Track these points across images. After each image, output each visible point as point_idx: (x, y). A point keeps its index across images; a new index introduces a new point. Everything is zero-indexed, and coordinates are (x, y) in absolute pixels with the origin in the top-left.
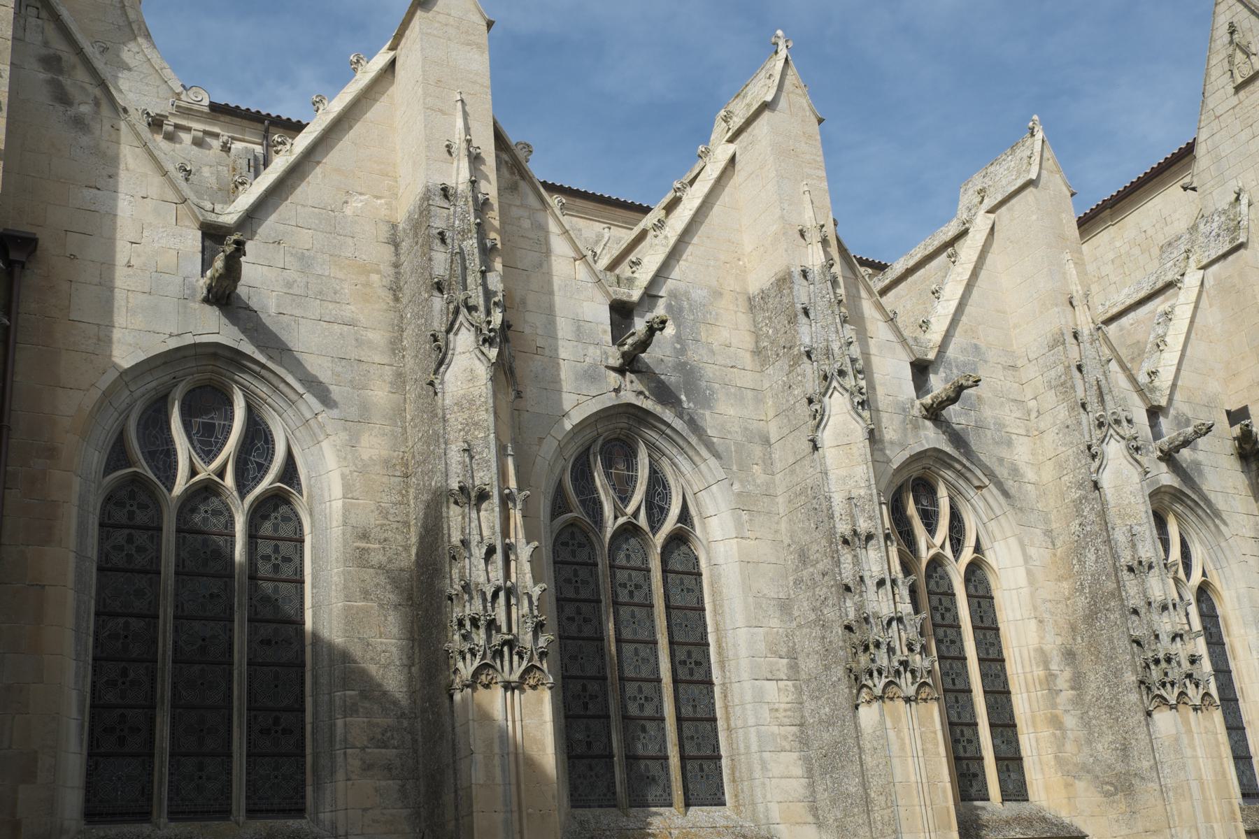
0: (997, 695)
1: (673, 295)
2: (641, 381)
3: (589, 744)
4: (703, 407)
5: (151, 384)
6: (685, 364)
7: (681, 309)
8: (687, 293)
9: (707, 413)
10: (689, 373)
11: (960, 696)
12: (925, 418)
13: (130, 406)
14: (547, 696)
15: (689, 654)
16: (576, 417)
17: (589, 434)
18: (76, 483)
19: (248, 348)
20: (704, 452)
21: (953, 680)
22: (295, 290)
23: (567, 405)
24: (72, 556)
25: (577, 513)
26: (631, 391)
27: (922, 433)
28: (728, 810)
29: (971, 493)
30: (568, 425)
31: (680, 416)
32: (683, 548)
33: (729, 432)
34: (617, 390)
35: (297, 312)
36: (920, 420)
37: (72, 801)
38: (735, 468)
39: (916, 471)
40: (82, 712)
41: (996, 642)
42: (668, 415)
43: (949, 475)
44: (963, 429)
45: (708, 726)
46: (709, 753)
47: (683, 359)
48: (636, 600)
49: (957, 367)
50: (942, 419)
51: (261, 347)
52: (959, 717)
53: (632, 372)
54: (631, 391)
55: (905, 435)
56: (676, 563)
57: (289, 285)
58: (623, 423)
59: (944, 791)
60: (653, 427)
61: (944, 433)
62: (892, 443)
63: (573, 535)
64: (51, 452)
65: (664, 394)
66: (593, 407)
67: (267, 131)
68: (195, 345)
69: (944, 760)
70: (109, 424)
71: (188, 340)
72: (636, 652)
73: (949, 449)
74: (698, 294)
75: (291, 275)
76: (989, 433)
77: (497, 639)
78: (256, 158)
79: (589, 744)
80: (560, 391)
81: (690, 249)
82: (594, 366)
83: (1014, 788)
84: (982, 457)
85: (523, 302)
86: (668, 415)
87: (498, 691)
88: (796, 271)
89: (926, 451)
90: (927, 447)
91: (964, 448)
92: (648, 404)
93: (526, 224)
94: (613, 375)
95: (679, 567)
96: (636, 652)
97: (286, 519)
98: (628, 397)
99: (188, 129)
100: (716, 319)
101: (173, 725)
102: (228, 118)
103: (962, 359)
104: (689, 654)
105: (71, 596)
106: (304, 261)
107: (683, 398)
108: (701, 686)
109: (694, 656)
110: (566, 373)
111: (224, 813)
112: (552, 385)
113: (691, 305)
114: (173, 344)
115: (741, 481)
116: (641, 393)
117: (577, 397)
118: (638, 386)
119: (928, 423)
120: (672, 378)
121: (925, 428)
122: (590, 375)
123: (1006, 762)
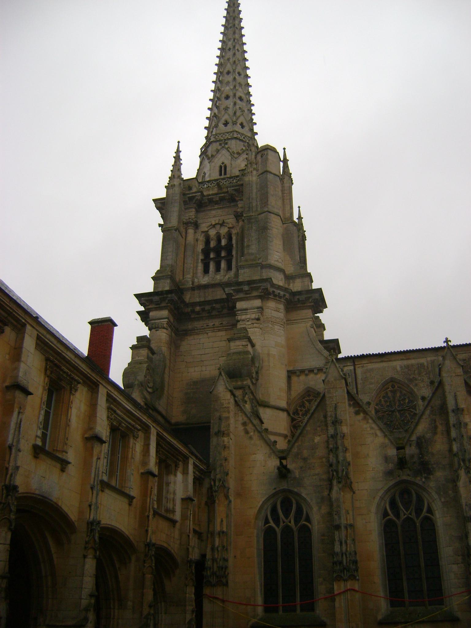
113: (425, 440)
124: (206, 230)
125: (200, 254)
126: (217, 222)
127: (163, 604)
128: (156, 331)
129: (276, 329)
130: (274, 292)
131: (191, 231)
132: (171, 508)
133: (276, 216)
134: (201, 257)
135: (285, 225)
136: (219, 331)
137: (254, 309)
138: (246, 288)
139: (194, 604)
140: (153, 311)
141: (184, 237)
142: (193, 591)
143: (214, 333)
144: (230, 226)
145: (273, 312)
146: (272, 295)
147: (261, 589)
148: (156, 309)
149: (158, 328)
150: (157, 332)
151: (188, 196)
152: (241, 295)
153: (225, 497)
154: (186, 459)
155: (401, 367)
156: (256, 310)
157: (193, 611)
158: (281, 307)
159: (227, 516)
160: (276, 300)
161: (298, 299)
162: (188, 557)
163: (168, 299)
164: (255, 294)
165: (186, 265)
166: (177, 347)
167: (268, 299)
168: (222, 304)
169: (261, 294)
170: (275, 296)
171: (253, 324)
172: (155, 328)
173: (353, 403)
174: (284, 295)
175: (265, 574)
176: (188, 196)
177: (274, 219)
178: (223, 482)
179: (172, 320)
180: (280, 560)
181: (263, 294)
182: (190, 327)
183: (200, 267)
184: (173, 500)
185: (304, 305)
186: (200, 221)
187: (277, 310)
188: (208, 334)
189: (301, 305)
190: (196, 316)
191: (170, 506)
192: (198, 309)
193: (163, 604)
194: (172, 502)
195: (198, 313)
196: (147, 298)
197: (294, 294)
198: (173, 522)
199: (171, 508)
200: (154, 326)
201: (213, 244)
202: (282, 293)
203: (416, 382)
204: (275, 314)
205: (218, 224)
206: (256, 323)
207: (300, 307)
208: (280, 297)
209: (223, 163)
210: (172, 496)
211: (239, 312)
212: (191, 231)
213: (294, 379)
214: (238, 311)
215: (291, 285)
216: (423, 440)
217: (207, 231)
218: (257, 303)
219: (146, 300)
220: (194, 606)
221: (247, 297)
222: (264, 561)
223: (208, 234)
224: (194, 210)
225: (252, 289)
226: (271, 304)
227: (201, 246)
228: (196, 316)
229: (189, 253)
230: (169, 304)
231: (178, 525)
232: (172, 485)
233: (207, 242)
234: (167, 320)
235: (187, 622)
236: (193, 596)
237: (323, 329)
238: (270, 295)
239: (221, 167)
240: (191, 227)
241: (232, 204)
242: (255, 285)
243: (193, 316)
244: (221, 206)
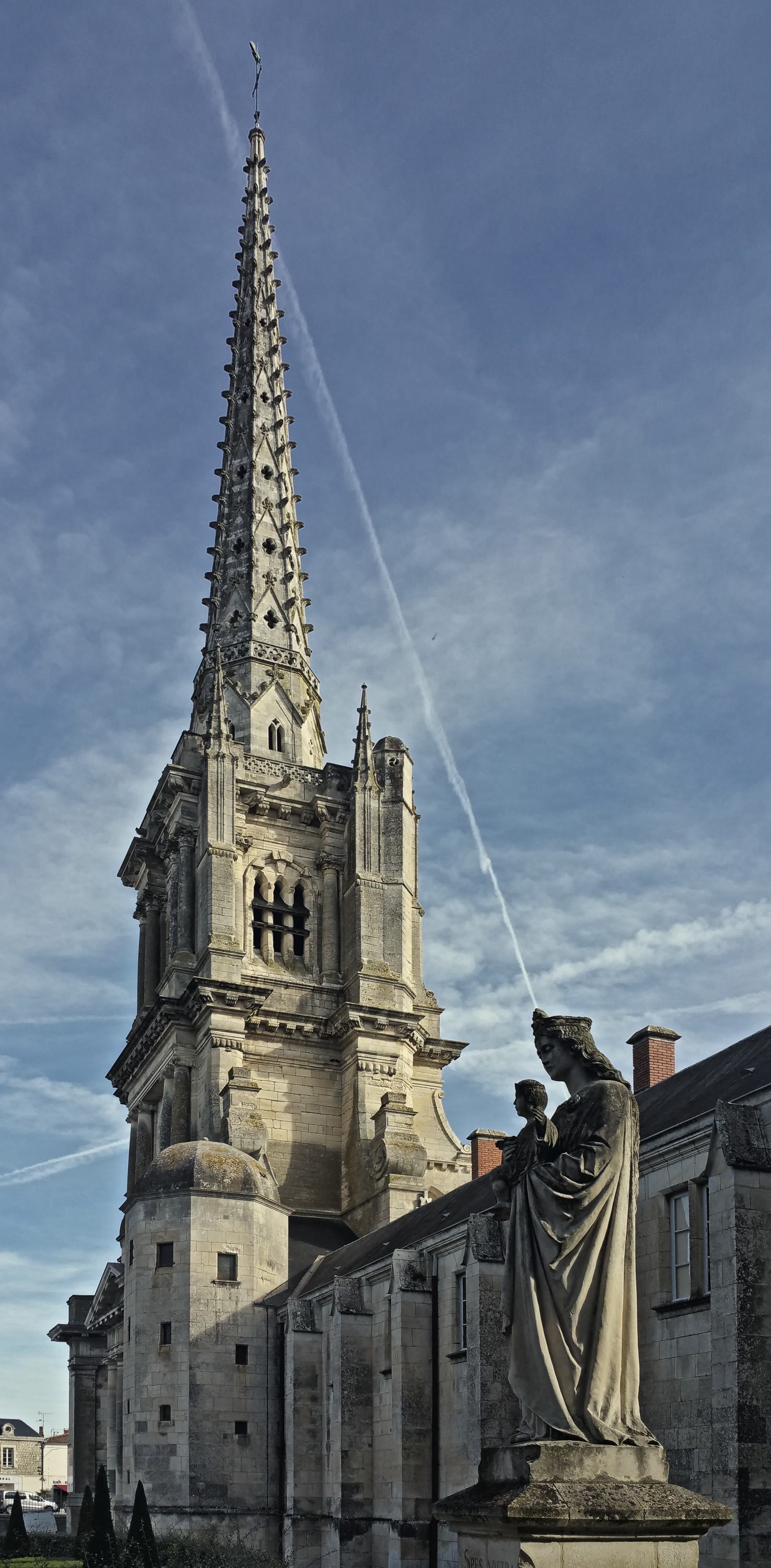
136: (301, 1067)
137: (386, 1056)
138: (382, 1020)
140: (217, 1012)
143: (292, 1068)
148: (225, 1012)
149: (232, 1047)
156: (389, 1058)
168: (318, 1027)
188: (281, 1067)
192: (274, 1022)
195: (272, 1029)
196: (214, 990)
209: (276, 722)
221: (376, 1034)
239: (271, 729)
241: (309, 829)
242: (396, 1020)
243: (259, 1032)
244: (290, 826)
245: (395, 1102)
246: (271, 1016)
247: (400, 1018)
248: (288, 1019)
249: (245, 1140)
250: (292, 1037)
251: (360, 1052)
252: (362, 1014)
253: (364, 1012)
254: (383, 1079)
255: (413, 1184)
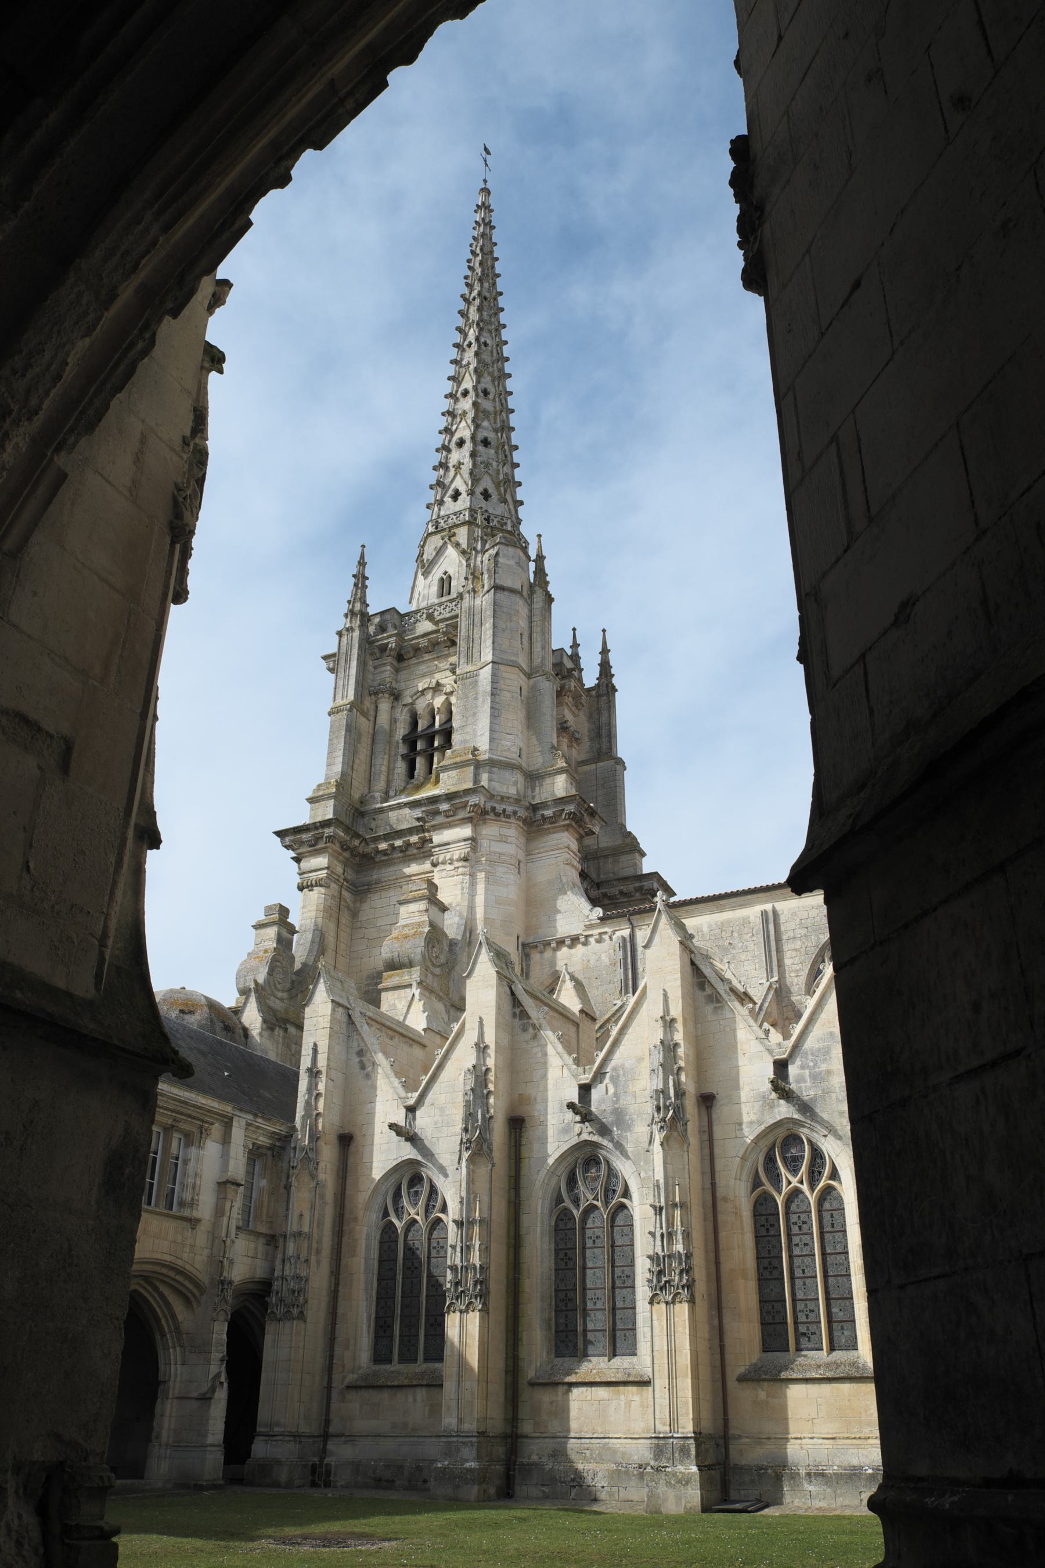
0: (839, 1278)
1: (615, 1069)
2: (591, 1127)
3: (566, 1325)
4: (626, 1132)
5: (393, 1180)
6: (618, 1109)
7: (618, 1076)
8: (622, 1066)
9: (628, 1134)
10: (619, 1114)
11: (808, 1281)
12: (780, 1098)
13: (387, 1192)
14: (477, 1314)
15: (623, 1272)
16: (556, 1155)
17: (570, 1159)
18: (365, 1230)
19: (420, 1158)
20: (623, 1159)
21: (803, 1271)
22: (439, 1125)
23: (550, 1150)
24: (363, 1261)
25: (568, 1203)
26: (588, 1133)
27: (776, 1110)
28: (634, 1359)
29: (823, 1139)
30: (551, 1161)
31: (612, 1141)
32: (625, 1211)
33: (640, 1142)
34: (579, 1134)
35: (439, 1135)
36: (776, 1101)
37: (365, 1356)
38: (642, 1164)
39: (781, 1133)
40: (369, 1320)
41: (843, 1241)
42: (605, 1142)
43: (805, 1131)
44: (811, 1099)
45: (630, 1311)
46: (630, 1327)
47: (616, 1106)
48: (596, 1245)
49: (812, 1054)
50: (795, 1095)
51: (423, 1156)
52: (805, 1293)
53: (588, 1121)
54: (588, 1133)
55: (763, 1115)
56: (620, 1220)
57: (436, 1123)
58: (589, 1149)
59: (686, 1355)
60: (602, 1149)
61: (794, 1106)
62: (751, 1122)
63: (565, 1215)
64: (356, 1219)
65: (604, 1130)
66: (565, 1147)
67: (629, 920)
68: (402, 1161)
69: (688, 1337)
70: (379, 1200)
71: (400, 1160)
72: (594, 1274)
73: (796, 1116)
74: (628, 1064)
75: (437, 1118)
76: (834, 1096)
77: (460, 1289)
78: (624, 939)
79: (566, 1325)
80: (547, 1143)
81: (627, 1036)
82: (569, 1124)
83: (846, 1341)
84: (825, 1116)
85: (535, 1099)
86: (605, 1142)
87: (458, 1314)
88: (651, 1046)
89: (780, 1120)
90: (779, 1118)
91: (810, 1112)
92: (596, 1138)
93: (539, 1055)
94: (578, 1125)
95: (622, 1223)
96: (594, 1274)
97: (442, 1229)
98: (585, 1137)
99: (592, 935)
100: (639, 1075)
101: (401, 1324)
102: (610, 921)
103: (817, 1046)
104: (623, 1272)
105: (362, 1277)
106: (442, 1109)
107: (615, 1129)
108: (629, 1289)
109: (626, 1272)
110: (551, 1132)
111: (415, 1360)
112: (544, 1140)
114: (395, 1163)
115: (645, 1171)
116: (592, 1132)
117: (557, 1144)
118: (590, 1129)
119: (782, 1102)
120: (608, 1119)
121: (779, 1105)
122: (566, 1130)
123: (841, 1324)
124: (410, 701)
125: (401, 745)
126: (426, 686)
127: (178, 1349)
128: (310, 891)
129: (498, 874)
130: (493, 809)
131: (384, 706)
132: (189, 1199)
133: (509, 669)
134: (403, 749)
135: (532, 681)
139: (225, 1349)
141: (372, 718)
142: (226, 1329)
144: (449, 689)
145: (493, 843)
146: (492, 814)
147: (369, 1326)
150: (311, 893)
151: (377, 644)
152: (440, 819)
153: (311, 1175)
154: (228, 1123)
155: (710, 926)
156: (463, 843)
157: (222, 1360)
158: (513, 832)
159: (313, 1207)
160: (501, 821)
161: (543, 815)
162: (221, 1275)
163: (326, 835)
164: (462, 814)
165: (373, 769)
166: (355, 914)
167: (485, 821)
169: (469, 815)
170: (497, 815)
171: (458, 868)
172: (308, 887)
173: (521, 1012)
174: (515, 813)
175: (379, 1298)
176: (377, 644)
177: (504, 675)
178: (306, 1152)
179: (339, 869)
180: (399, 1278)
181: (473, 814)
182: (375, 877)
183: (401, 767)
184: (194, 1188)
185: (553, 825)
186: (402, 685)
187: (503, 839)
189: (549, 826)
190: (383, 858)
191: (188, 1196)
193: (178, 1349)
194: (190, 1190)
195: (384, 853)
196: (292, 838)
197: (535, 808)
198: (193, 1223)
199: (189, 1199)
200: (305, 884)
201: (422, 725)
202: (510, 809)
203: (734, 951)
204: (498, 848)
205: (429, 688)
206: (462, 867)
207: (548, 829)
208: (509, 817)
209: (445, 573)
210: (190, 1181)
211: (437, 849)
212: (384, 706)
213: (535, 956)
214: (434, 847)
215: (537, 789)
216: (621, 1072)
217: (412, 704)
218: (467, 831)
219: (292, 841)
220: (225, 1353)
221: (449, 823)
222: (378, 1280)
223: (415, 708)
224: (389, 668)
225: (455, 810)
226: (491, 830)
227: (402, 730)
228: (383, 858)
229: (380, 747)
230: (328, 845)
231: (204, 1227)
232: (192, 1164)
233: (414, 723)
234: (326, 871)
235: (211, 1377)
236: (225, 1336)
237: (637, 855)
238: (488, 814)
240: (383, 700)
244: (435, 656)
245: (416, 891)
246: (378, 840)
247: (461, 797)
248: (394, 839)
249: (247, 978)
250: (407, 853)
251: (434, 847)
252: (424, 809)
253: (425, 805)
254: (458, 868)
255: (406, 977)
